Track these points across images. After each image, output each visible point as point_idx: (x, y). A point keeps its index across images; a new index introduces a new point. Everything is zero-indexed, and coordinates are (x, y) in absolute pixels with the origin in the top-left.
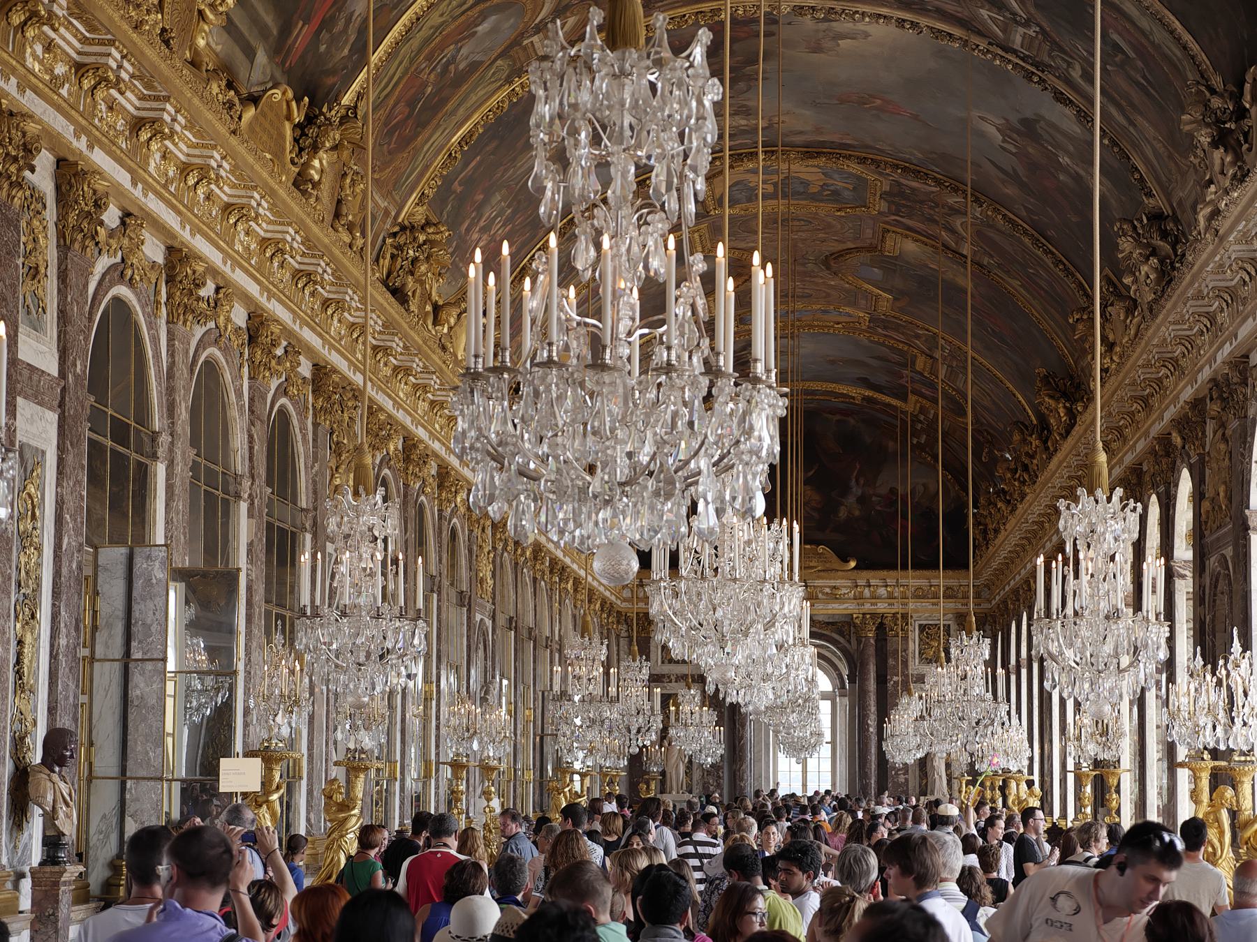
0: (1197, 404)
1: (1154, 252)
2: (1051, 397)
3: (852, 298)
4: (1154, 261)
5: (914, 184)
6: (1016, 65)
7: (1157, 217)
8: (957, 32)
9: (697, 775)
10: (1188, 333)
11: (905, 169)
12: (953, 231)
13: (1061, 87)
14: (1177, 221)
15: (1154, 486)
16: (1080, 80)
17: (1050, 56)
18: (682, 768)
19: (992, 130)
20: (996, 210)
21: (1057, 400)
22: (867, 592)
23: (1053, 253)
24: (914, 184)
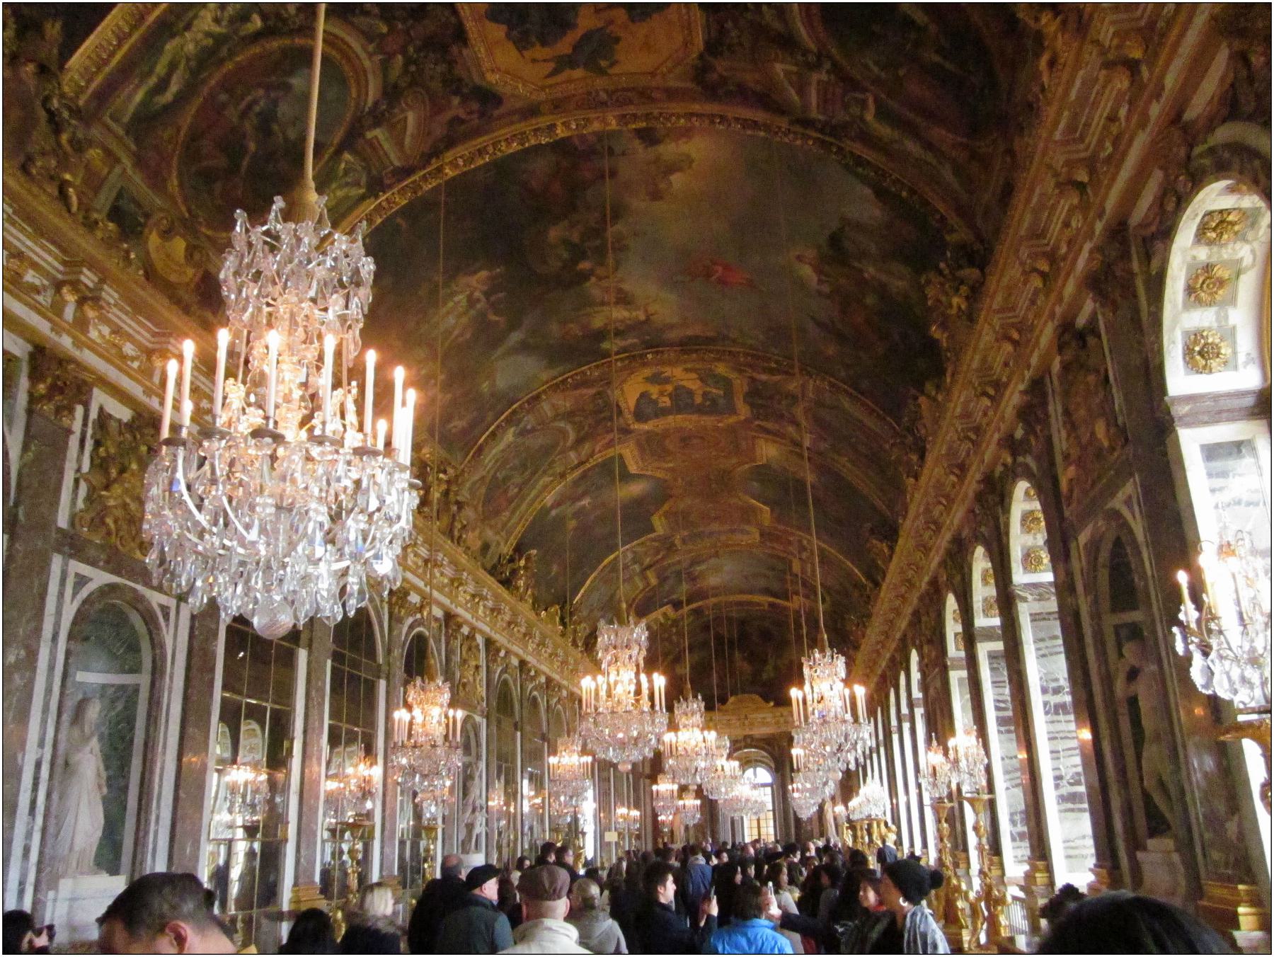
0: (1037, 387)
3: (747, 514)
5: (764, 377)
6: (816, 140)
8: (760, 116)
9: (691, 832)
11: (753, 356)
12: (795, 423)
13: (858, 148)
15: (978, 538)
17: (846, 106)
18: (682, 829)
19: (807, 271)
20: (823, 379)
21: (881, 541)
22: (782, 720)
24: (764, 377)
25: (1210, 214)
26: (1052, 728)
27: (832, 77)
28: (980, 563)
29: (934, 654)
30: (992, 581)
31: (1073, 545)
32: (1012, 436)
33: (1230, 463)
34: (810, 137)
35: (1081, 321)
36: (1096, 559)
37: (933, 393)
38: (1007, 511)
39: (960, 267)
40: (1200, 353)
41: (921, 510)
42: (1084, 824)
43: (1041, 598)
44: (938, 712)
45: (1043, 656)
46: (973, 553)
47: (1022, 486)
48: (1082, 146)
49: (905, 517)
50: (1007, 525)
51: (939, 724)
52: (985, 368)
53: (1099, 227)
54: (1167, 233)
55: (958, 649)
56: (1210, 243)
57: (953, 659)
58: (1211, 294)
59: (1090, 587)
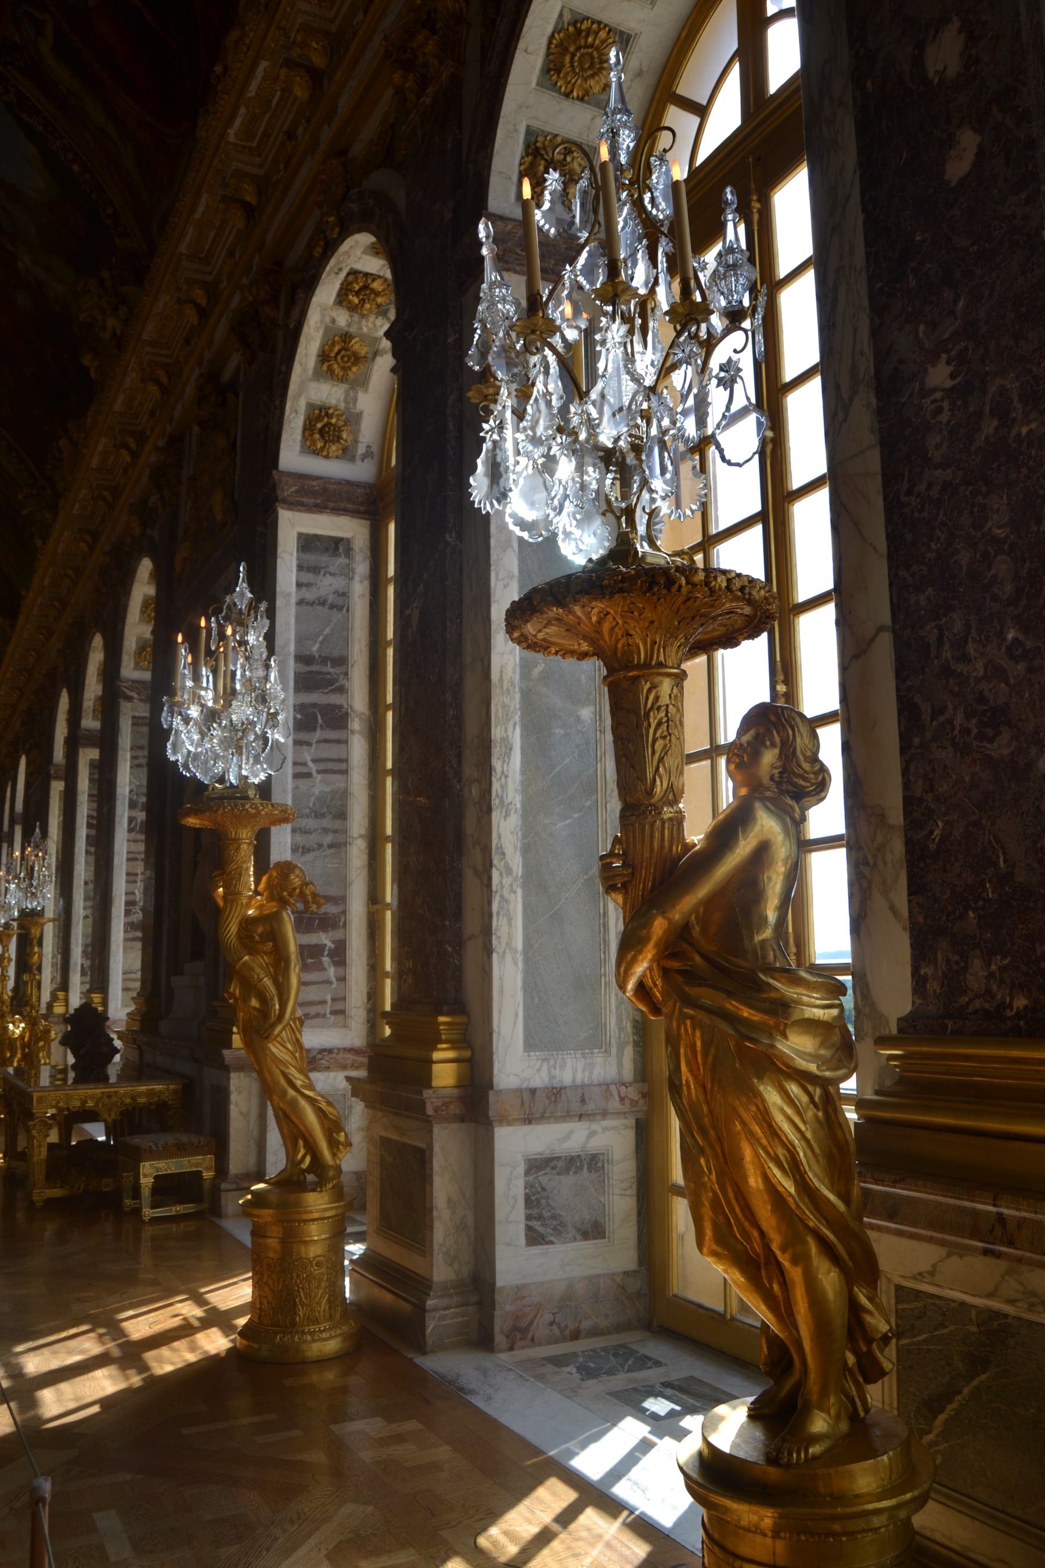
25: (353, 273)
33: (324, 559)
35: (226, 375)
38: (128, 593)
40: (321, 432)
54: (311, 284)
56: (352, 309)
58: (343, 368)
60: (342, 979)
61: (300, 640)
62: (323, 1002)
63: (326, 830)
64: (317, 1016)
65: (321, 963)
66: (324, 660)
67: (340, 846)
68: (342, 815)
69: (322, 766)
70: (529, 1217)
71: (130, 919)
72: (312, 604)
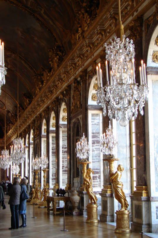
0: (69, 86)
1: (58, 55)
2: (26, 98)
4: (58, 57)
6: (28, 11)
7: (58, 47)
10: (67, 70)
14: (63, 47)
15: (53, 110)
16: (43, 15)
19: (19, 32)
23: (29, 65)
26: (63, 156)
27: (35, 2)
28: (53, 115)
29: (38, 133)
30: (55, 119)
31: (71, 121)
32: (63, 92)
33: (95, 117)
34: (27, 10)
36: (75, 126)
37: (47, 73)
38: (60, 107)
39: (57, 51)
40: (94, 98)
41: (40, 97)
42: (66, 176)
43: (65, 127)
44: (37, 148)
45: (64, 140)
46: (51, 112)
47: (63, 104)
48: (82, 51)
49: (35, 97)
50: (60, 110)
51: (37, 152)
52: (60, 75)
53: (83, 67)
55: (44, 133)
57: (43, 135)
59: (73, 130)
60: (100, 181)
61: (92, 130)
62: (97, 184)
63: (97, 159)
64: (96, 186)
65: (97, 179)
66: (96, 133)
67: (99, 161)
68: (99, 157)
69: (96, 149)
70: (118, 208)
71: (63, 170)
72: (94, 125)
